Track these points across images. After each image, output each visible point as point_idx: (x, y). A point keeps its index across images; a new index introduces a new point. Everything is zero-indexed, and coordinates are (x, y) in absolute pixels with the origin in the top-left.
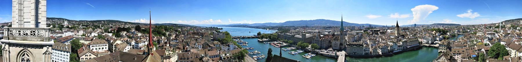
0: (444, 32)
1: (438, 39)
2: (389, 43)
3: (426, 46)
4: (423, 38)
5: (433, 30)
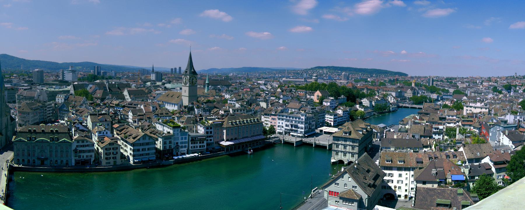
0: (352, 97)
1: (329, 118)
2: (159, 127)
3: (289, 144)
4: (282, 114)
5: (312, 88)
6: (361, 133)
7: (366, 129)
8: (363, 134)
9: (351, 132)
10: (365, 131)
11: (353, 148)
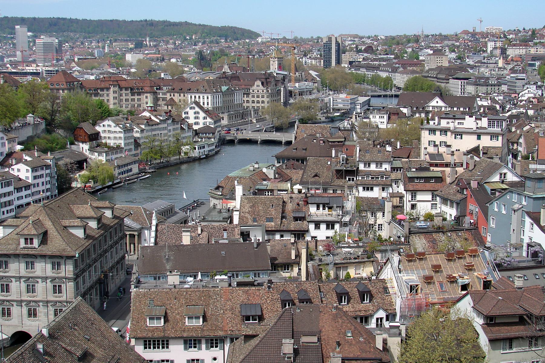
6: (79, 233)
7: (99, 220)
8: (88, 237)
9: (45, 234)
10: (93, 224)
11: (57, 289)
